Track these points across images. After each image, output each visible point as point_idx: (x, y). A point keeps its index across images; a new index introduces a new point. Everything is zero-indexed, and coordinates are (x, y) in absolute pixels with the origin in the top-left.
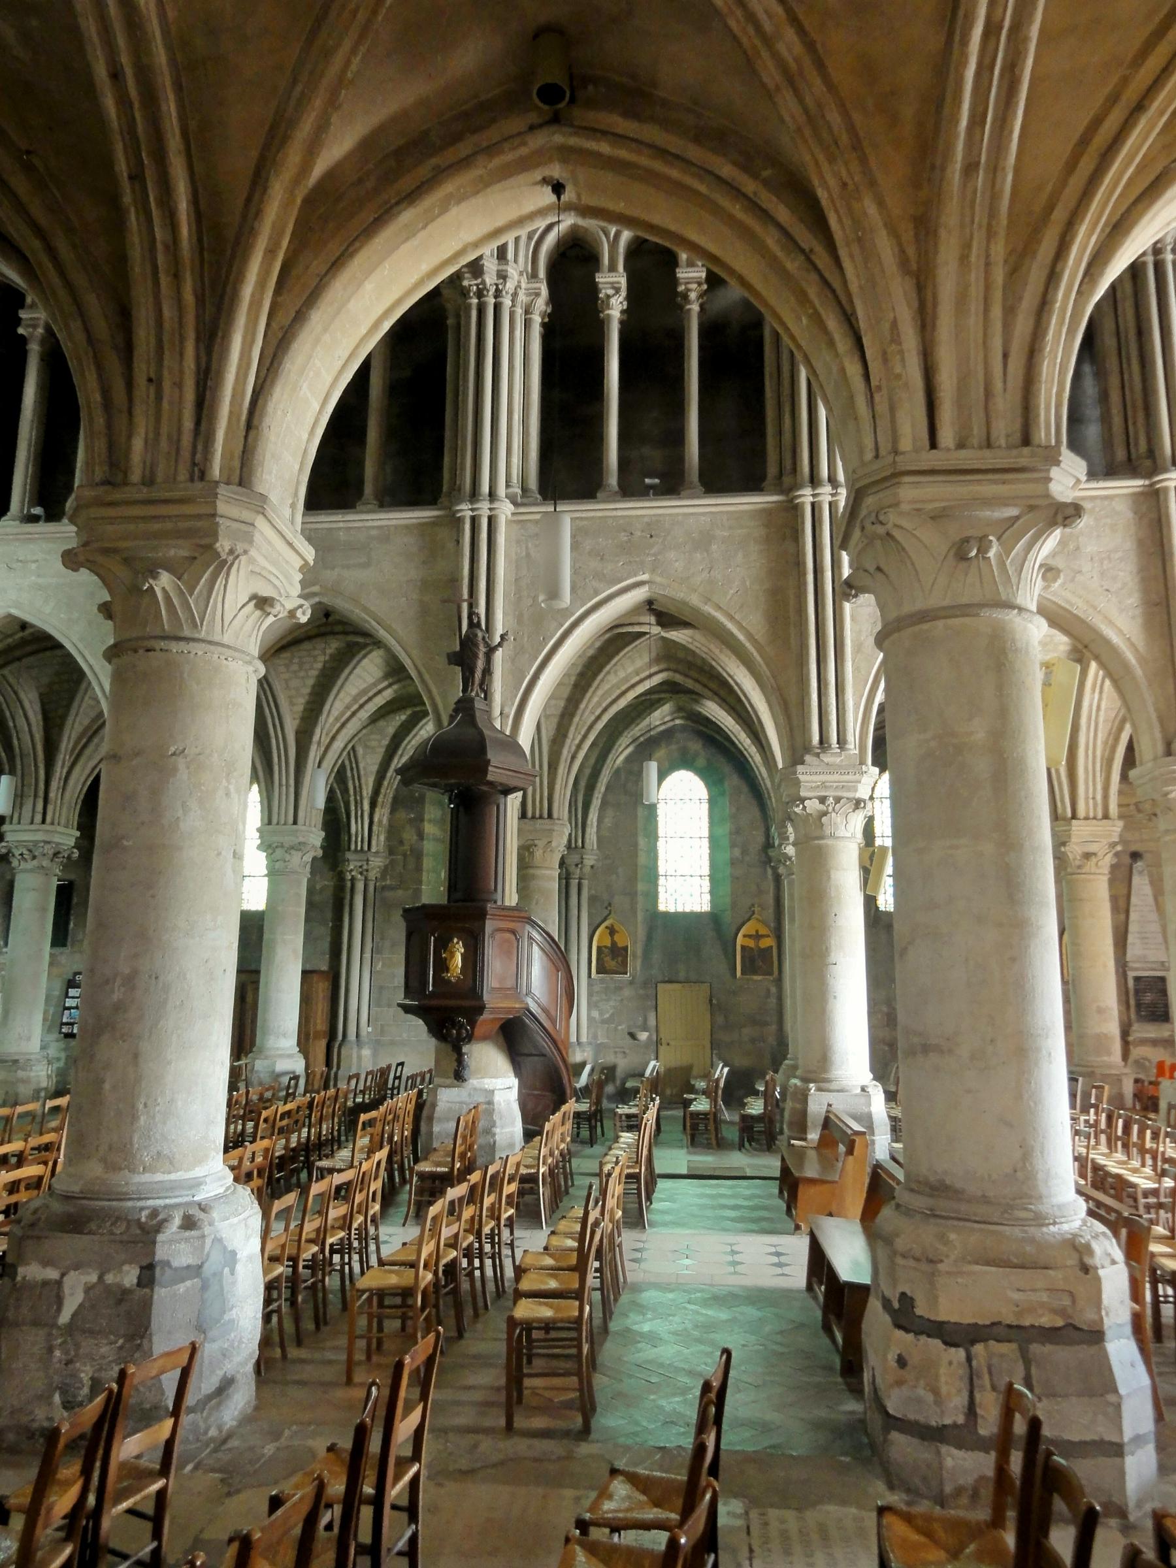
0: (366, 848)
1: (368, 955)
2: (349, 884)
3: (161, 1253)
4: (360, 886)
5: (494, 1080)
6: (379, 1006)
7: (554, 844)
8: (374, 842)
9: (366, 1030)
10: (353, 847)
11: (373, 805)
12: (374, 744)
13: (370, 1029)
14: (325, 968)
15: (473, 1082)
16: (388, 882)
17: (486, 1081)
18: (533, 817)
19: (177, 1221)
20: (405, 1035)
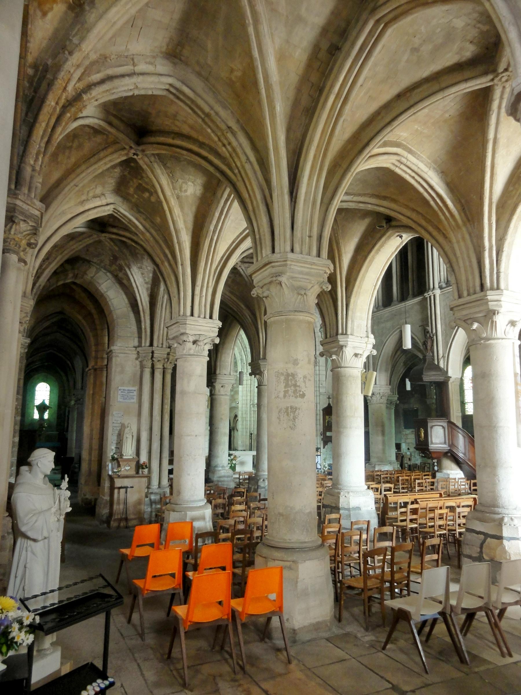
3: (259, 484)
15: (445, 471)
19: (262, 480)
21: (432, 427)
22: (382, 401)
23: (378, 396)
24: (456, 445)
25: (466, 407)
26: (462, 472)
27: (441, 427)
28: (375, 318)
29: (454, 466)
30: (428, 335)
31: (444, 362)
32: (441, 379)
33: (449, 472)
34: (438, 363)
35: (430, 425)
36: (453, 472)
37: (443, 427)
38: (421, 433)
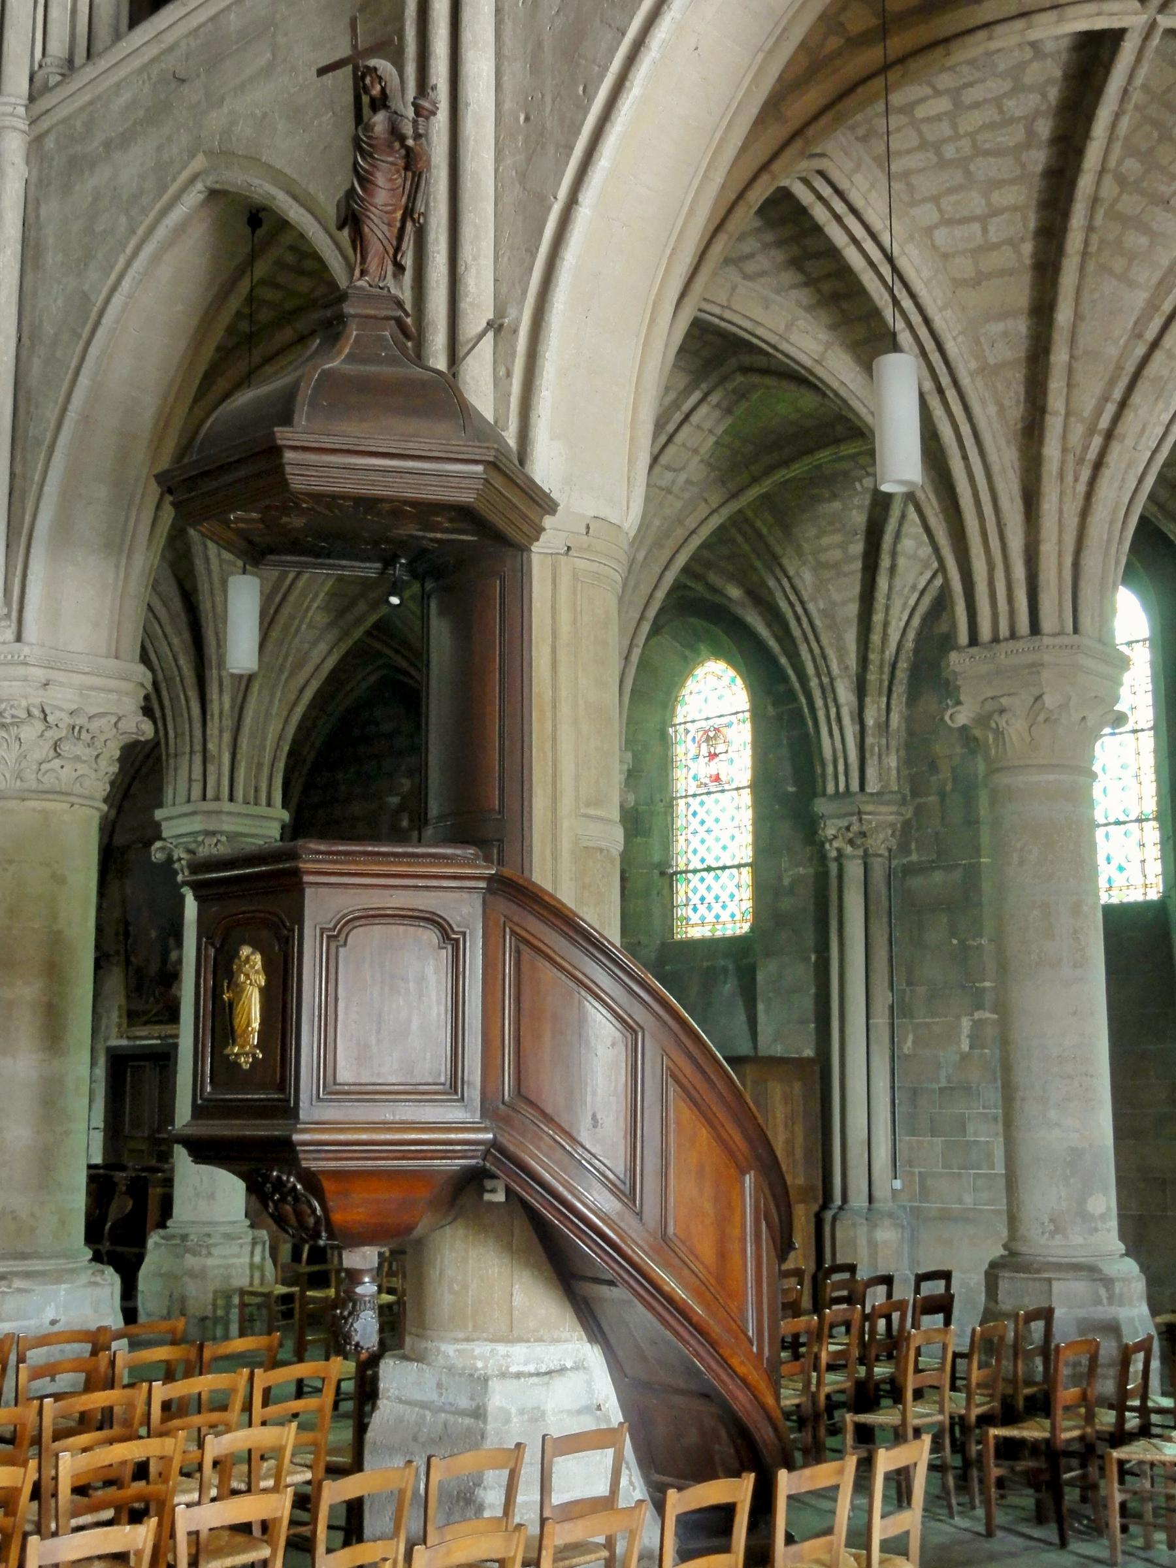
0: (855, 786)
1: (881, 1021)
2: (833, 867)
4: (854, 870)
5: (502, 1349)
6: (913, 1132)
7: (1049, 701)
8: (871, 772)
9: (885, 1183)
10: (830, 789)
11: (861, 690)
12: (835, 555)
13: (898, 1184)
14: (809, 1052)
15: (449, 1350)
16: (914, 857)
17: (481, 1349)
18: (996, 639)
20: (968, 1199)
21: (335, 936)
22: (64, 774)
23: (30, 732)
24: (552, 1101)
25: (680, 898)
26: (593, 1355)
27: (431, 936)
28: (50, 144)
29: (530, 1297)
30: (379, 121)
31: (500, 382)
32: (457, 480)
33: (485, 1355)
34: (453, 358)
35: (321, 906)
36: (519, 1356)
37: (450, 938)
38: (238, 990)
